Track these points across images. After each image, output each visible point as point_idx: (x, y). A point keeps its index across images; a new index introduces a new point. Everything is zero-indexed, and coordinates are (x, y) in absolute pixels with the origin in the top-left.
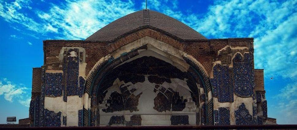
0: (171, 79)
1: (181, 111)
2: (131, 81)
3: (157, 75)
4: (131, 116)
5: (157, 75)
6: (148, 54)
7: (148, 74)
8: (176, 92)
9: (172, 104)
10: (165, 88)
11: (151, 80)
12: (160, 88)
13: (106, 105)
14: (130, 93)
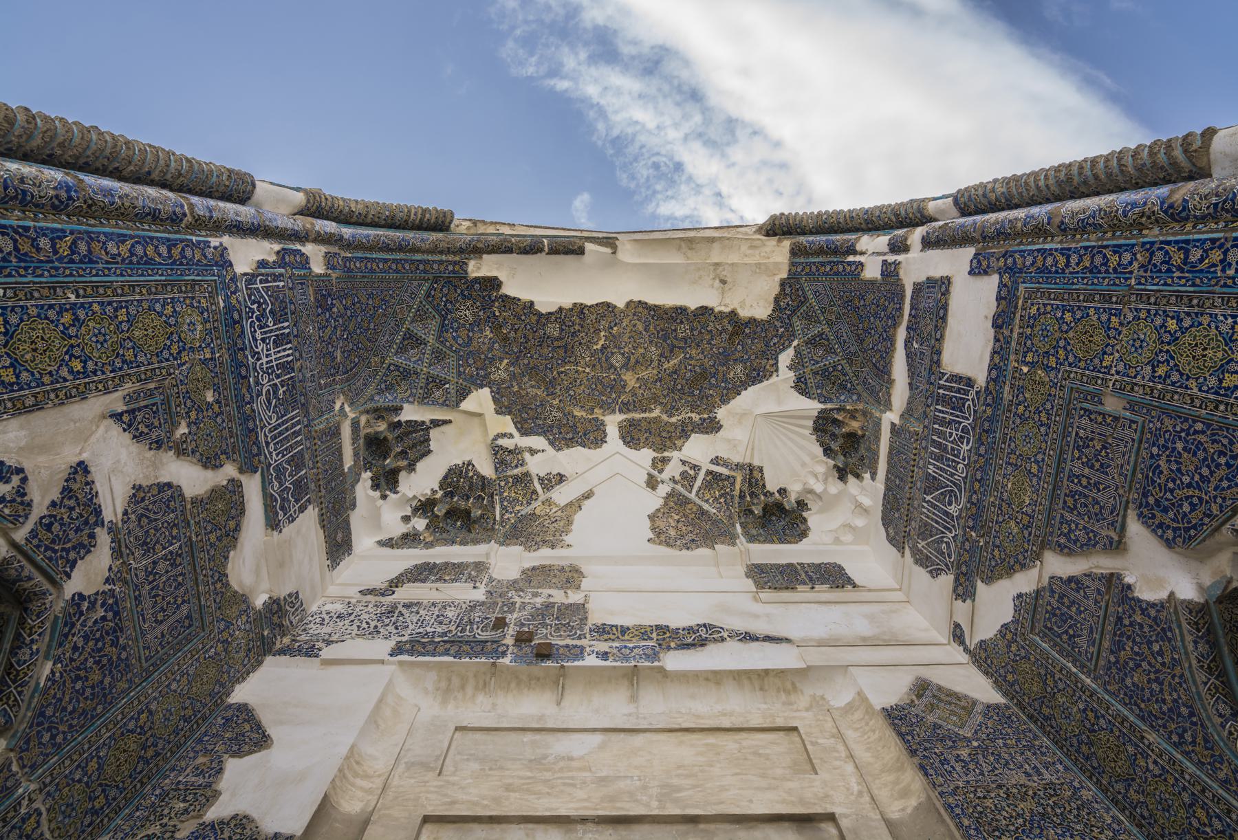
0: (721, 413)
1: (789, 542)
2: (544, 433)
3: (656, 413)
4: (527, 565)
5: (656, 413)
6: (618, 290)
7: (621, 411)
8: (751, 468)
9: (738, 526)
10: (696, 468)
11: (631, 435)
12: (674, 469)
13: (406, 519)
14: (535, 492)
